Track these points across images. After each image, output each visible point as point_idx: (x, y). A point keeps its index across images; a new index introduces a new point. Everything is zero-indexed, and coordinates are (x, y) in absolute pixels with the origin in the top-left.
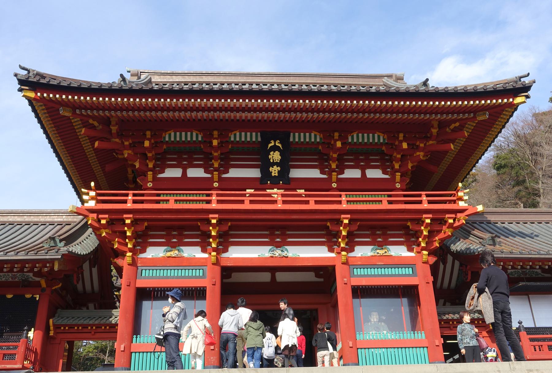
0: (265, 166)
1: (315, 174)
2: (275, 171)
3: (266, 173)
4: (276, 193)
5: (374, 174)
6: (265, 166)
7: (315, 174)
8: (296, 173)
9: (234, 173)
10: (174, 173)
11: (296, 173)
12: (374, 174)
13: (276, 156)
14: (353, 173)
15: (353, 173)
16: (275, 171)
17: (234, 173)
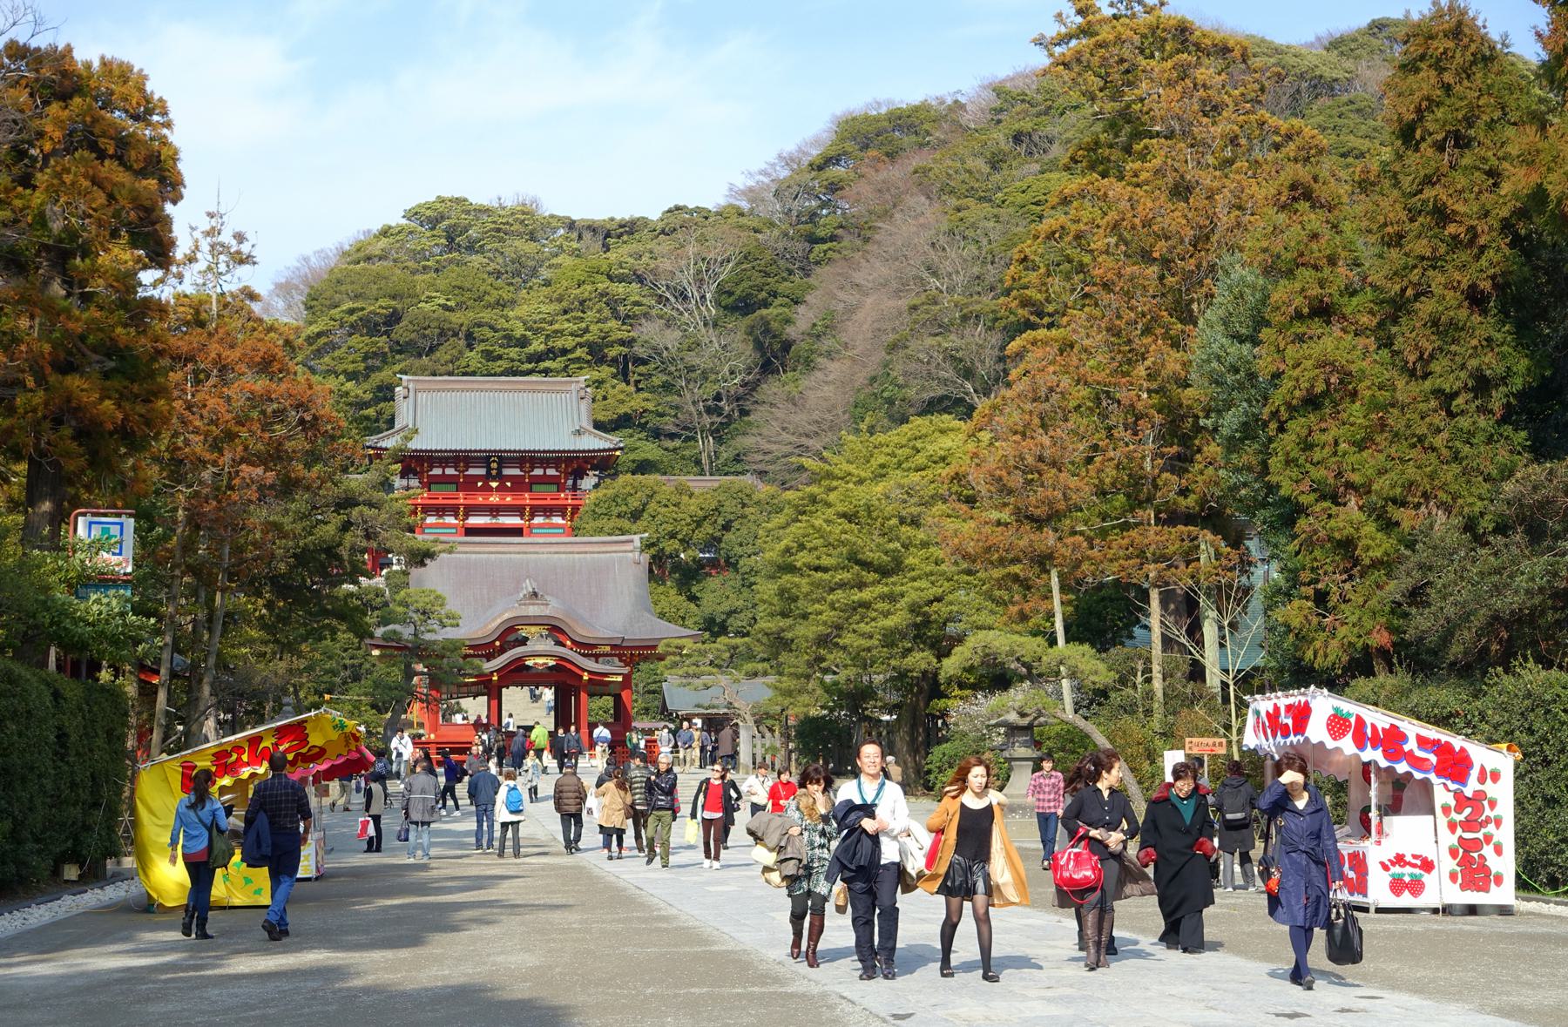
0: (489, 469)
1: (517, 472)
2: (494, 472)
3: (489, 472)
4: (494, 484)
5: (551, 472)
6: (489, 469)
7: (517, 472)
8: (506, 472)
9: (471, 471)
10: (437, 471)
11: (506, 472)
12: (551, 472)
13: (494, 465)
14: (538, 472)
15: (538, 472)
16: (494, 472)
17: (471, 471)
